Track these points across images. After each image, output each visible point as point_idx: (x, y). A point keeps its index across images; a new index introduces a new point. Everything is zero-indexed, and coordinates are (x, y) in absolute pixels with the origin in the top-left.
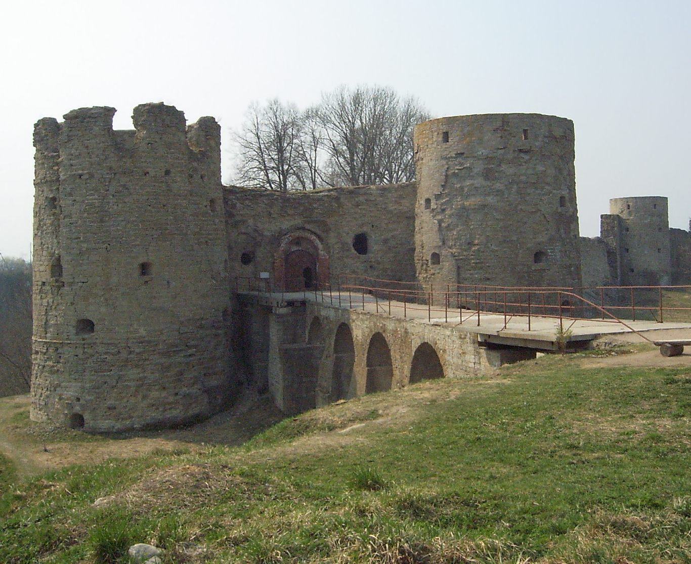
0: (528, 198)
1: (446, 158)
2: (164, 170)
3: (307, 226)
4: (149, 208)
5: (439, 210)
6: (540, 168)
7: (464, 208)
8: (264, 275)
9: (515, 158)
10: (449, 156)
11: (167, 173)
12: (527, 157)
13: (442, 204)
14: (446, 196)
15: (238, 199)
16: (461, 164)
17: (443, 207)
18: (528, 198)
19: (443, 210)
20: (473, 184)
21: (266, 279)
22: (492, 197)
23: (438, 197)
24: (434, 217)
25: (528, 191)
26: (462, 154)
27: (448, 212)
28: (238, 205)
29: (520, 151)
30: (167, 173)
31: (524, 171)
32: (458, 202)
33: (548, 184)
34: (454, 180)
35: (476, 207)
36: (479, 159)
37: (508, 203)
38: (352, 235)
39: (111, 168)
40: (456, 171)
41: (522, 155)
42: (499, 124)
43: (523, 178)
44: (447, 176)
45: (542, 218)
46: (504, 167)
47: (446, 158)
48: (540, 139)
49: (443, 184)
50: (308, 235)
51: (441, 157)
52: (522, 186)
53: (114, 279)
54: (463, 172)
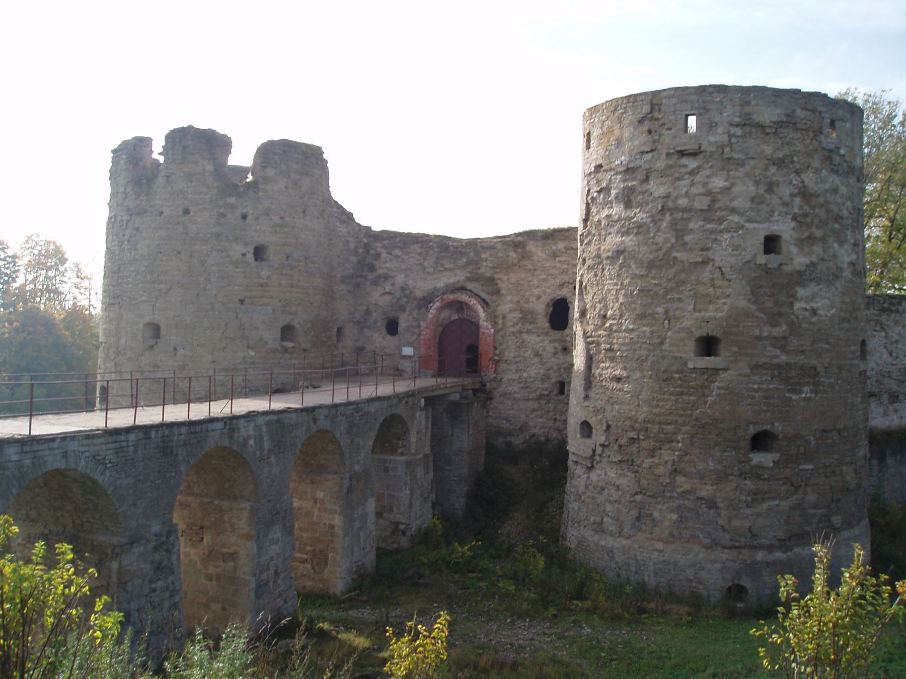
0: (688, 238)
2: (181, 209)
3: (470, 286)
4: (159, 256)
6: (718, 183)
8: (408, 351)
9: (671, 166)
11: (187, 212)
12: (692, 164)
15: (384, 247)
18: (688, 238)
20: (609, 216)
21: (410, 357)
25: (692, 225)
28: (384, 255)
29: (682, 154)
30: (187, 212)
31: (684, 190)
33: (733, 210)
35: (610, 254)
36: (617, 173)
37: (654, 247)
38: (546, 299)
39: (129, 210)
41: (684, 161)
42: (646, 109)
43: (683, 202)
45: (717, 274)
46: (652, 185)
48: (720, 130)
50: (463, 297)
52: (679, 215)
53: (123, 341)
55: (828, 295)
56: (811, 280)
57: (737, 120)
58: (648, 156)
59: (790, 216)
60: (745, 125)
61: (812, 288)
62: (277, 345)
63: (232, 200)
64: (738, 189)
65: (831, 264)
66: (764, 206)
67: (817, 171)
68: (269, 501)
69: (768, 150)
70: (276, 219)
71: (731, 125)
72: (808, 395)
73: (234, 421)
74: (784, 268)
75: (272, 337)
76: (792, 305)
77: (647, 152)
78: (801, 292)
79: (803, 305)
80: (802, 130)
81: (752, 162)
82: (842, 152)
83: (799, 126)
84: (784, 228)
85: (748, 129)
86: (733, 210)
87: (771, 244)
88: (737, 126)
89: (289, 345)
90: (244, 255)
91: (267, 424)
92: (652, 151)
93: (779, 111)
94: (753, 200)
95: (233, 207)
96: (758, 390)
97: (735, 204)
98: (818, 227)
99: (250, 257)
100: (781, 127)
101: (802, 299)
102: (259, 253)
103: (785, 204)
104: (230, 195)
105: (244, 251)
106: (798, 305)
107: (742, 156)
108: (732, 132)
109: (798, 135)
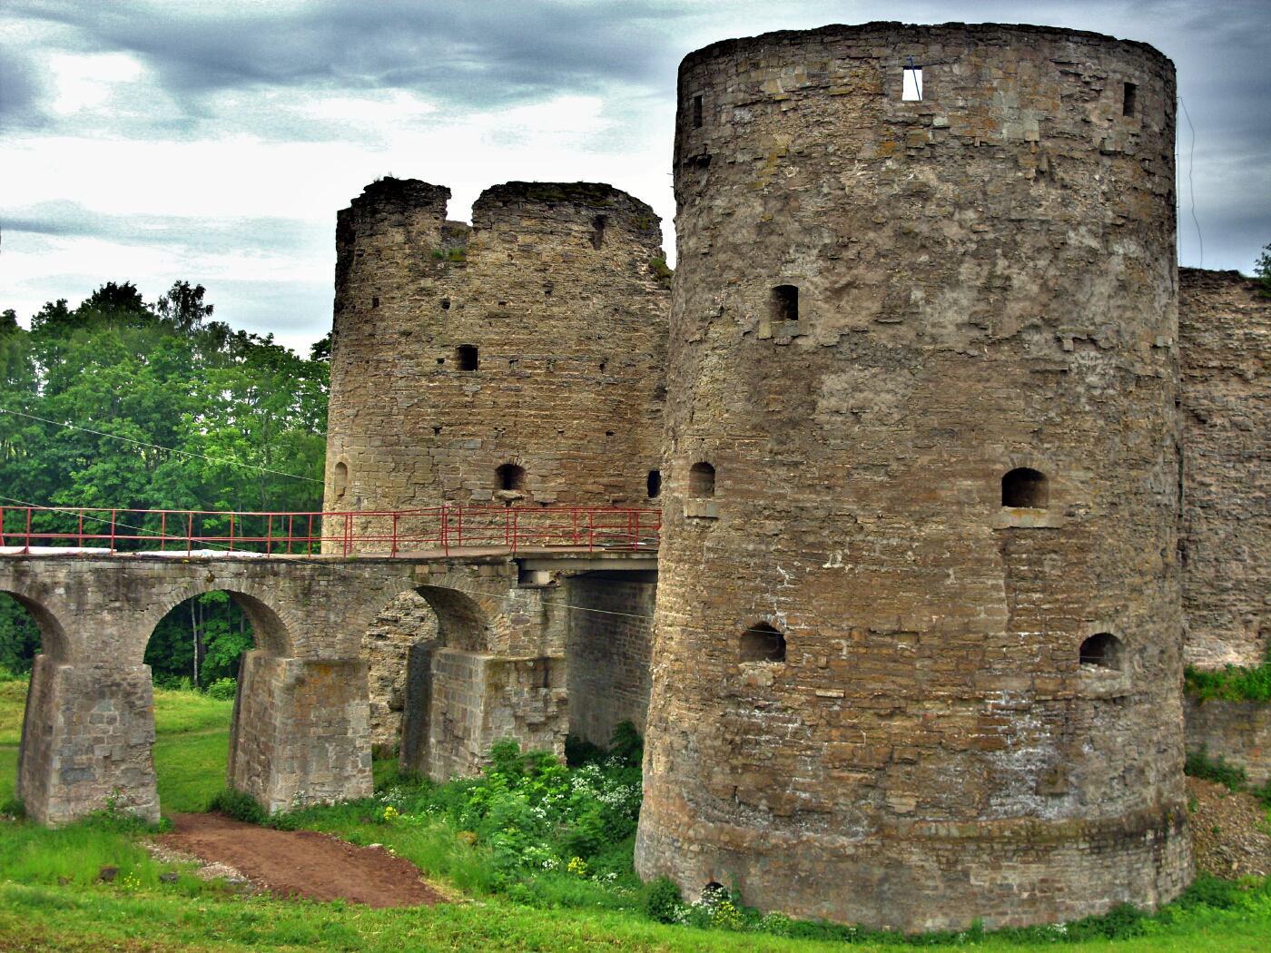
48: (724, 118)
55: (890, 386)
56: (853, 361)
57: (741, 96)
59: (815, 252)
60: (754, 103)
61: (856, 372)
62: (488, 494)
63: (427, 283)
64: (742, 212)
65: (903, 329)
66: (774, 238)
67: (871, 164)
68: (96, 668)
69: (782, 140)
70: (493, 306)
71: (736, 106)
72: (836, 566)
73: (26, 563)
74: (799, 341)
75: (481, 484)
76: (813, 406)
78: (831, 382)
79: (833, 402)
80: (841, 95)
81: (759, 164)
82: (938, 121)
83: (834, 90)
84: (806, 272)
85: (758, 108)
86: (735, 248)
87: (787, 300)
88: (744, 106)
89: (513, 494)
90: (441, 361)
91: (96, 571)
93: (799, 70)
94: (760, 227)
95: (429, 293)
96: (752, 556)
97: (738, 239)
98: (870, 266)
99: (451, 364)
100: (806, 97)
101: (832, 394)
102: (468, 357)
103: (807, 230)
104: (424, 275)
105: (442, 356)
106: (822, 403)
107: (748, 158)
108: (738, 118)
109: (837, 105)
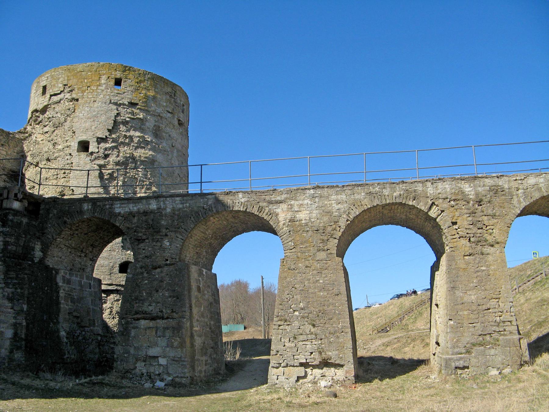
1: (116, 104)
5: (101, 154)
7: (133, 158)
10: (121, 102)
13: (106, 149)
14: (112, 142)
16: (132, 113)
17: (106, 153)
19: (106, 156)
22: (160, 154)
23: (100, 140)
24: (92, 161)
26: (137, 104)
27: (112, 159)
32: (126, 151)
34: (122, 128)
40: (128, 119)
44: (115, 122)
47: (116, 104)
49: (111, 128)
51: (111, 101)
54: (135, 121)
58: (169, 115)
77: (169, 112)
92: (171, 113)
